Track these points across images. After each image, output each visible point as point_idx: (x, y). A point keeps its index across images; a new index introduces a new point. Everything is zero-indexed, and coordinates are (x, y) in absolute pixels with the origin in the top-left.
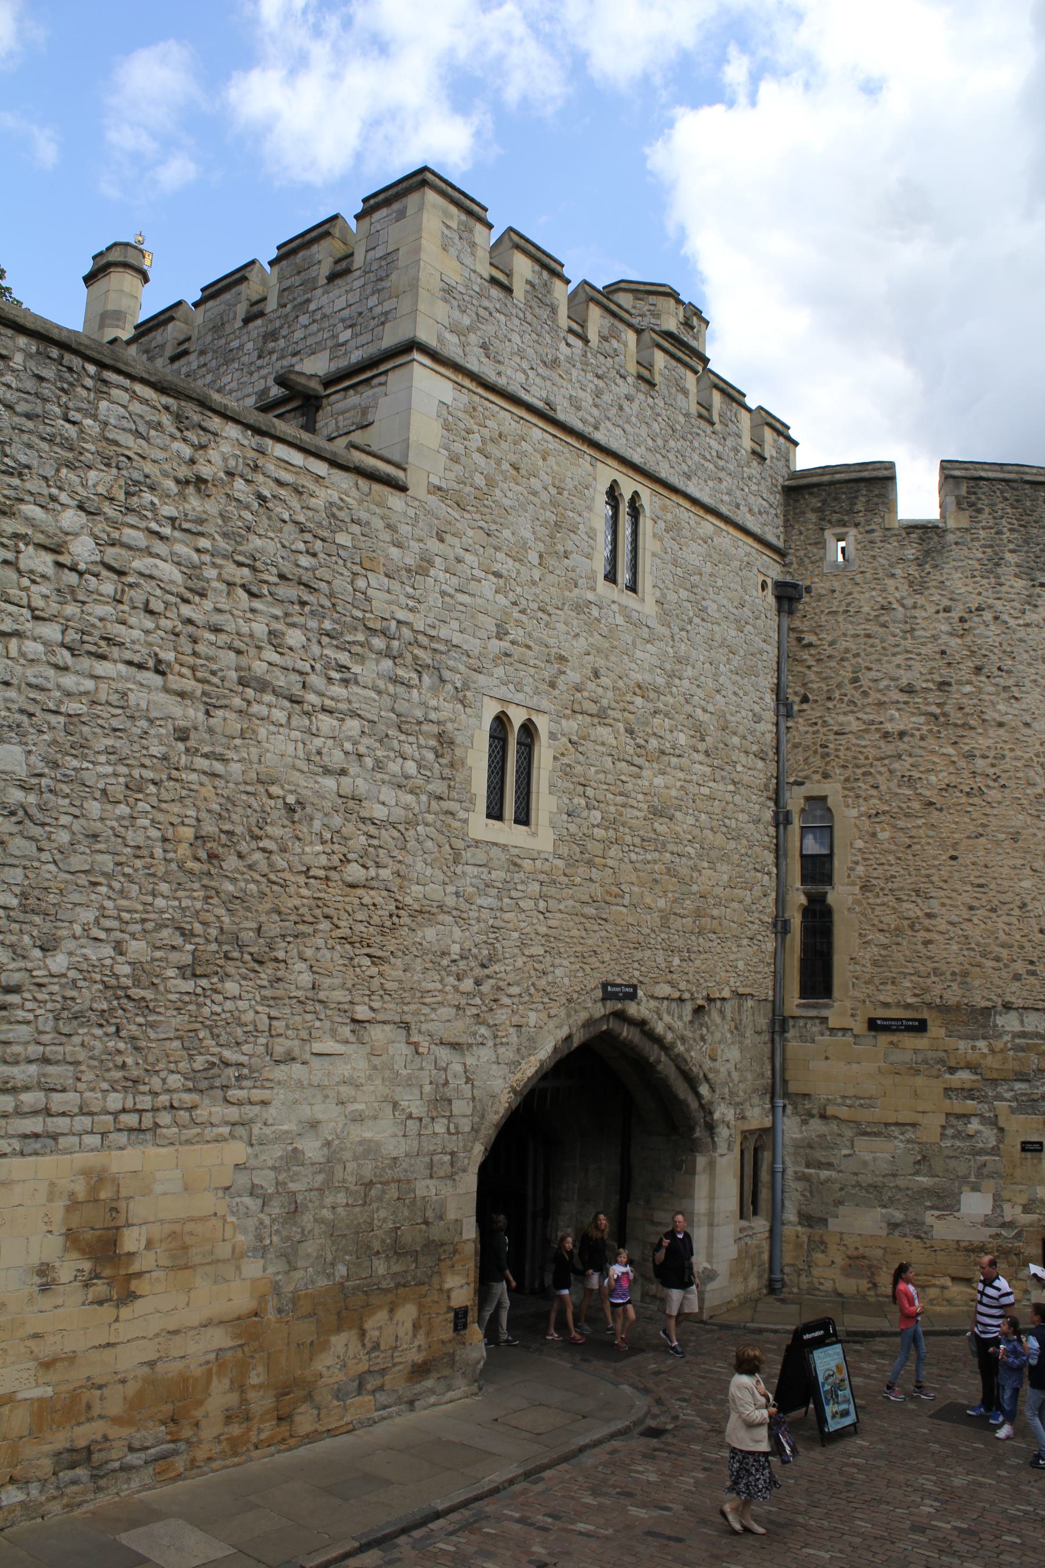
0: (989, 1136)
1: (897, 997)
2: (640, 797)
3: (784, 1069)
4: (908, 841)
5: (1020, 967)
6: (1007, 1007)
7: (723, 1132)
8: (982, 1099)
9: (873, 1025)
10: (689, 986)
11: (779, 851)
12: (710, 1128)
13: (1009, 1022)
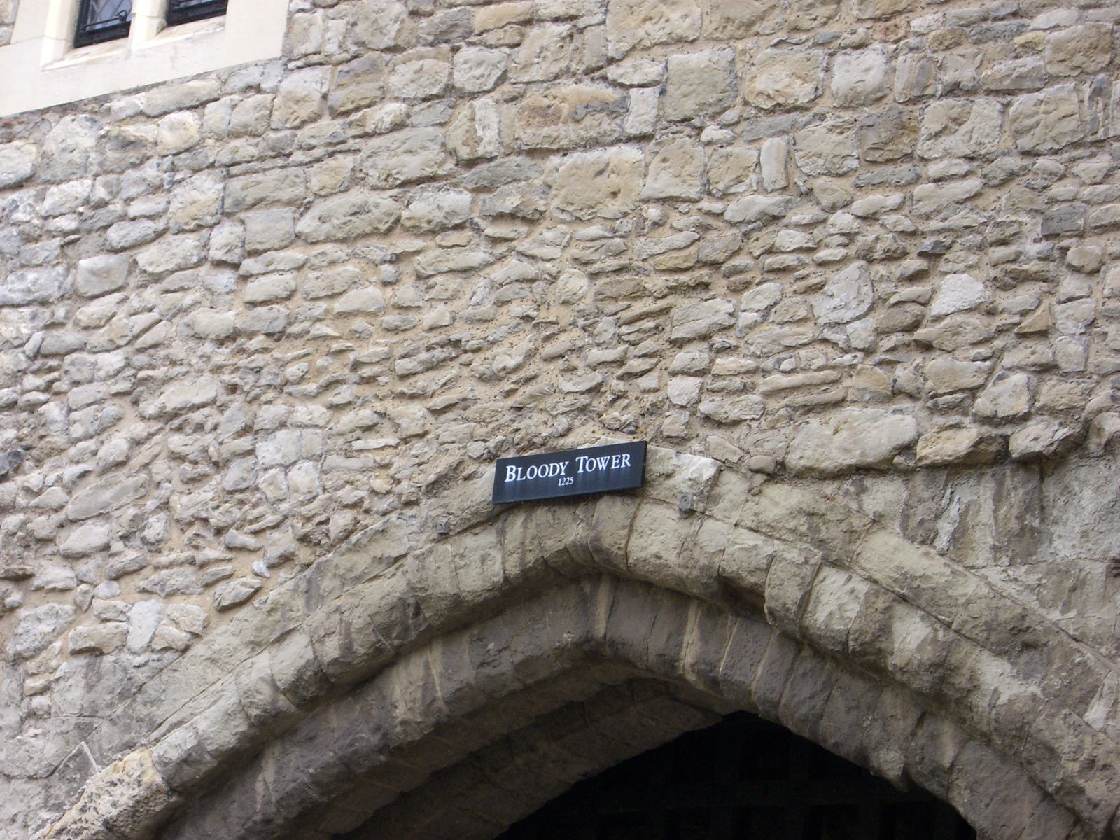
10: (1054, 391)
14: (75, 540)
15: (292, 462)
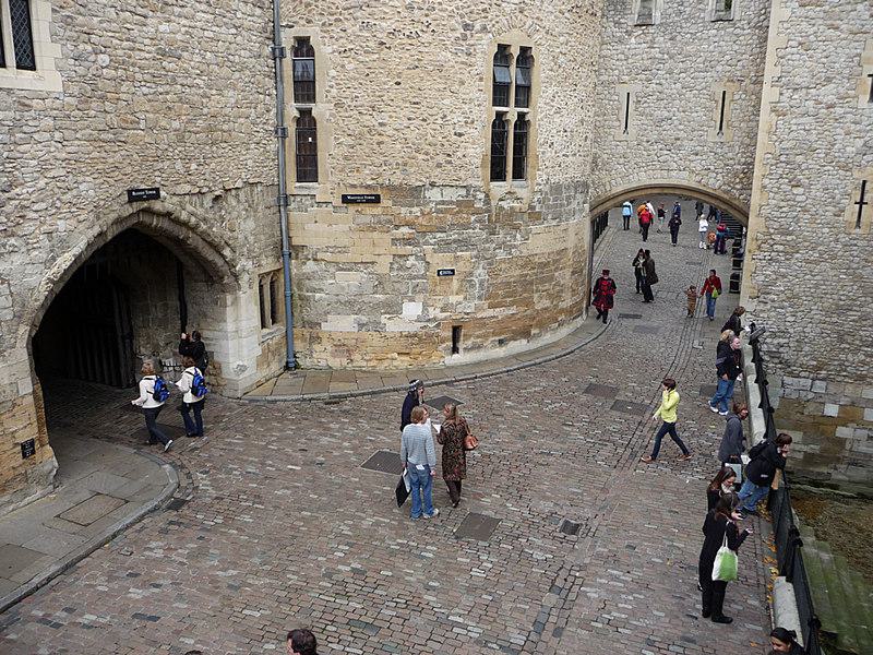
0: (421, 265)
1: (362, 180)
2: (147, 41)
3: (288, 229)
4: (367, 71)
5: (441, 159)
6: (433, 185)
7: (245, 278)
8: (417, 245)
9: (345, 199)
10: (207, 183)
11: (277, 77)
12: (236, 277)
13: (434, 195)
14: (36, 207)
15: (87, 188)
